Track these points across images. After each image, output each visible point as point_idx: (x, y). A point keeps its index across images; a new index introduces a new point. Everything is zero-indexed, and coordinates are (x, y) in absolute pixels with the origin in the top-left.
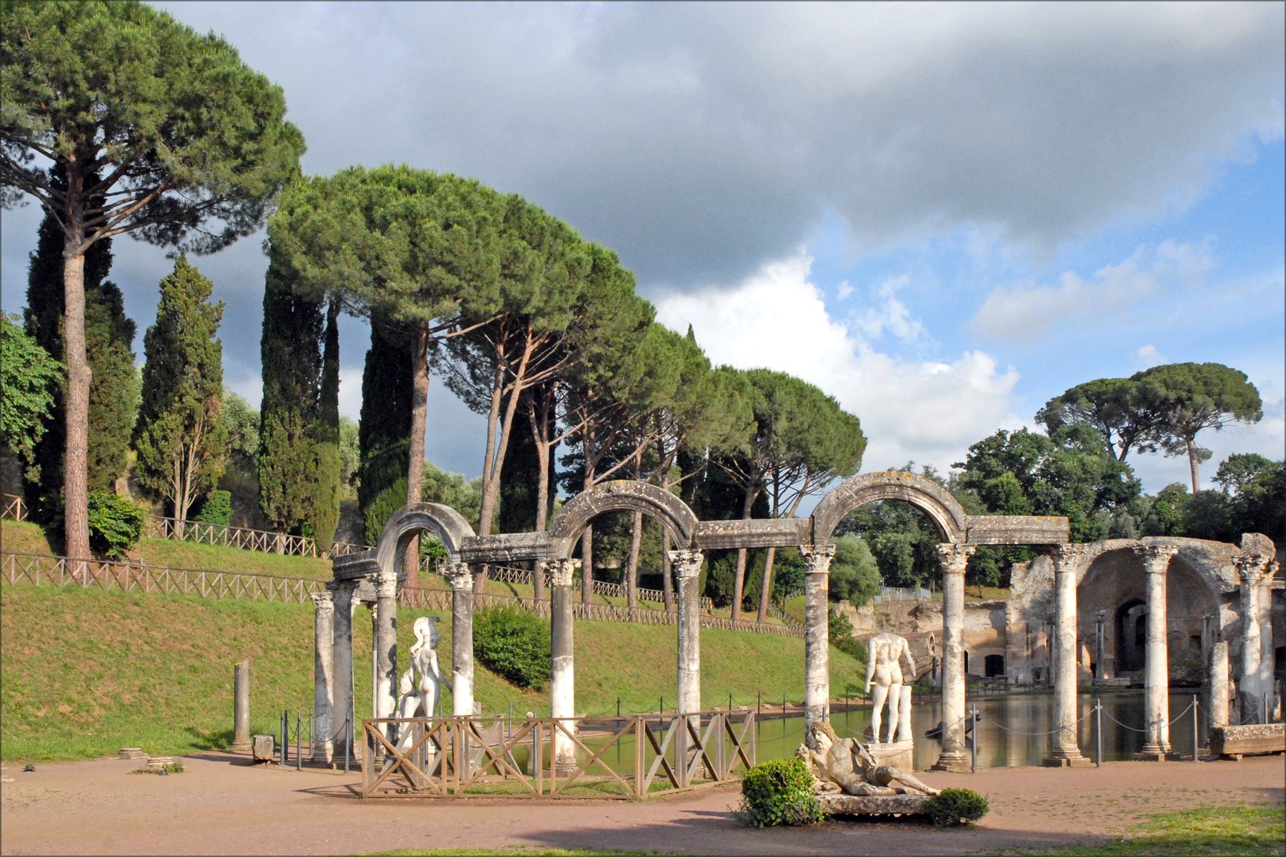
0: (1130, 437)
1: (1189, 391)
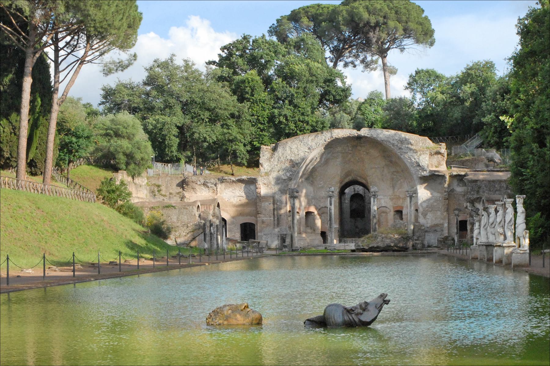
0: (338, 54)
1: (385, 17)
